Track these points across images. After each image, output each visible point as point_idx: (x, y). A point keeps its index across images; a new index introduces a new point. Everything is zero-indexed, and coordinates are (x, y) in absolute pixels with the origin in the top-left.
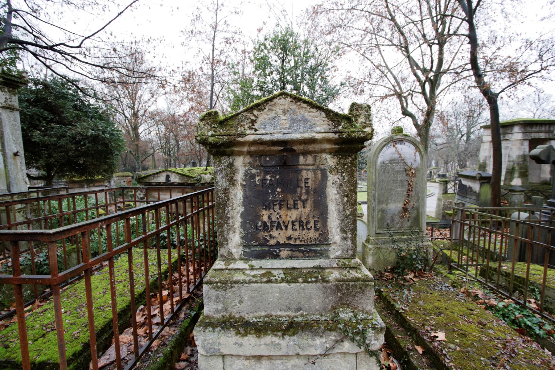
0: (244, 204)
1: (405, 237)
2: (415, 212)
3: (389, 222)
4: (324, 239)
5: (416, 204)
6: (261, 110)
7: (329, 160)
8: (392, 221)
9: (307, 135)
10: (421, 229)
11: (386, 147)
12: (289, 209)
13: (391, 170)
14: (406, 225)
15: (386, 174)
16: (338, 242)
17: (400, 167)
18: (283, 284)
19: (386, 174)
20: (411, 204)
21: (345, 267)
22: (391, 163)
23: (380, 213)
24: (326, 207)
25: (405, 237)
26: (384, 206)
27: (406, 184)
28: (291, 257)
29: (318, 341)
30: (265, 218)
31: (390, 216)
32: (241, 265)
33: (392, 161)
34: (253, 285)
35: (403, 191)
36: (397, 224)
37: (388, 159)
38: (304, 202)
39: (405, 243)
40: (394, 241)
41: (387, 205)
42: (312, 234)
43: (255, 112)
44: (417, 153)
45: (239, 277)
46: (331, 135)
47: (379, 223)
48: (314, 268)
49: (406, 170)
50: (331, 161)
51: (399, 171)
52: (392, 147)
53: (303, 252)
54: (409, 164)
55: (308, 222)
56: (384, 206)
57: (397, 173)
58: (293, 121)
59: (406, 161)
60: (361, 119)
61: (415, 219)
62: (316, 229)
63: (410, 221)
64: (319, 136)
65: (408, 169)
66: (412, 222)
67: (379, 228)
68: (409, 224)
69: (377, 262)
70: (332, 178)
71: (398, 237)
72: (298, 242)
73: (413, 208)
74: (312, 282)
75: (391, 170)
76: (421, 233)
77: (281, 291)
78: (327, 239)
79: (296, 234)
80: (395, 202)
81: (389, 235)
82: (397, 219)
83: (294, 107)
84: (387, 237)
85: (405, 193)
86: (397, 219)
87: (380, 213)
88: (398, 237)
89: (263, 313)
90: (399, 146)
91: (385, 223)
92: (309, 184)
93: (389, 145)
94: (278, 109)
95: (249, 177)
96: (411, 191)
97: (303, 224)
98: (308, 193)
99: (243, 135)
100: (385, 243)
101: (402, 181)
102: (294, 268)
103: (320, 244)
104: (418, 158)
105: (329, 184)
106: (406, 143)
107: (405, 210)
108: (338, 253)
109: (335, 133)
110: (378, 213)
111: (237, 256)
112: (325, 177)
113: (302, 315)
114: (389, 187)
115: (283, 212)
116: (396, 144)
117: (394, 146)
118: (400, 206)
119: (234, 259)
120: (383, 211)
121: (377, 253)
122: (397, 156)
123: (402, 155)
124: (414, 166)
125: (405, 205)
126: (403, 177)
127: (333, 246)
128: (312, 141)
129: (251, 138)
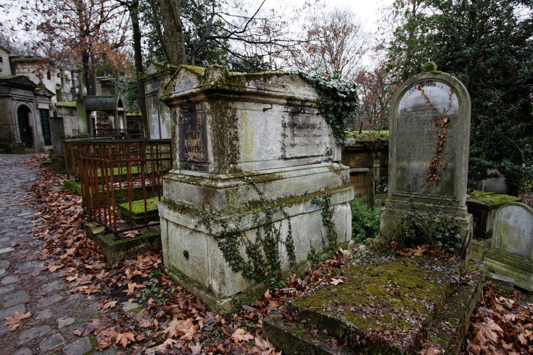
0: (179, 137)
1: (431, 205)
2: (449, 174)
3: (411, 183)
4: (206, 161)
5: (449, 164)
6: (176, 79)
7: (207, 106)
8: (415, 183)
9: (190, 91)
10: (455, 197)
11: (408, 91)
12: (193, 138)
13: (414, 120)
14: (434, 191)
15: (408, 124)
16: (212, 162)
17: (428, 115)
18: (186, 184)
19: (408, 124)
20: (442, 163)
21: (212, 179)
22: (414, 111)
23: (399, 172)
24: (207, 137)
25: (431, 205)
26: (405, 163)
27: (436, 137)
28: (195, 170)
29: (193, 221)
30: (186, 145)
31: (412, 177)
32: (177, 172)
33: (417, 108)
34: (177, 182)
35: (431, 146)
36: (421, 187)
37: (411, 106)
38: (199, 134)
39: (428, 212)
40: (413, 208)
41: (409, 163)
42: (202, 156)
43: (175, 80)
44: (454, 96)
45: (174, 178)
46: (198, 89)
47: (397, 184)
48: (200, 177)
49: (436, 119)
50: (208, 106)
51: (427, 120)
52: (418, 91)
53: (199, 167)
54: (441, 111)
55: (200, 147)
56: (405, 163)
57: (424, 122)
58: (186, 83)
59: (437, 107)
60: (210, 77)
61: (447, 184)
62: (204, 153)
63: (440, 186)
64: (194, 91)
65: (440, 117)
66: (442, 188)
67: (398, 189)
68: (439, 189)
69: (389, 227)
70: (209, 118)
71: (421, 203)
72: (197, 161)
73: (444, 169)
74: (194, 184)
75: (414, 120)
76: (455, 204)
77: (186, 189)
78: (207, 159)
79: (196, 155)
80: (419, 159)
81: (408, 199)
82: (421, 181)
83: (186, 74)
84: (405, 202)
85: (434, 149)
86: (421, 181)
87: (399, 172)
88: (421, 203)
89: (180, 200)
90: (427, 89)
91: (406, 185)
92: (200, 123)
93: (413, 88)
94: (181, 77)
95: (181, 119)
96: (442, 146)
97: (198, 148)
98: (199, 128)
99: (171, 94)
100: (401, 207)
101: (429, 133)
102: (193, 176)
103: (204, 163)
104: (455, 102)
105: (207, 122)
106: (437, 83)
107: (433, 170)
108: (212, 170)
109: (200, 87)
110: (397, 171)
111: (178, 167)
112: (205, 117)
113: (192, 205)
114: (412, 141)
115: (191, 140)
116: (423, 86)
117: (420, 89)
118: (426, 165)
119: (177, 169)
120: (403, 170)
121: (389, 217)
122: (423, 101)
123: (431, 100)
124: (449, 113)
125: (433, 164)
126: (431, 127)
127: (211, 165)
128: (193, 95)
129: (173, 96)
